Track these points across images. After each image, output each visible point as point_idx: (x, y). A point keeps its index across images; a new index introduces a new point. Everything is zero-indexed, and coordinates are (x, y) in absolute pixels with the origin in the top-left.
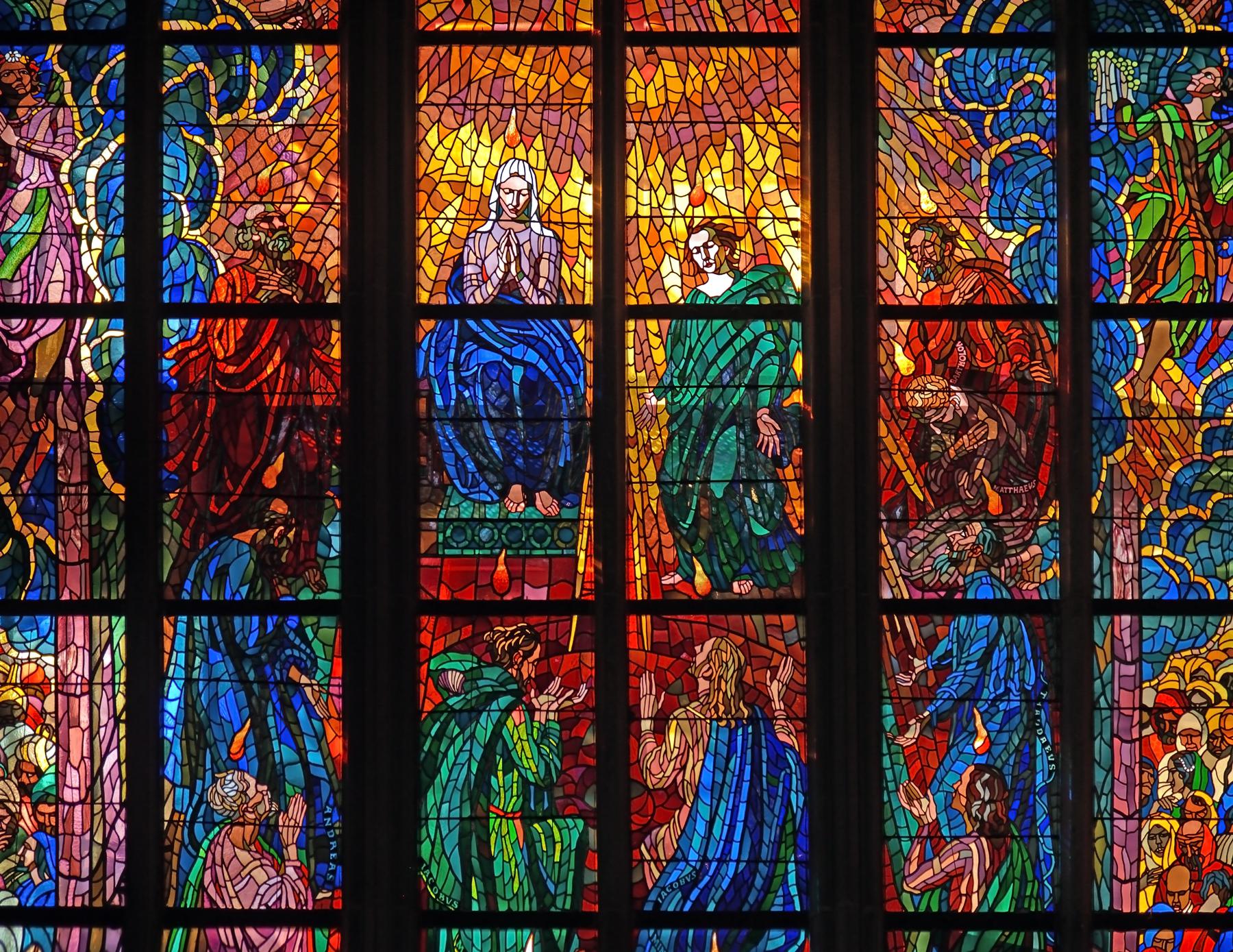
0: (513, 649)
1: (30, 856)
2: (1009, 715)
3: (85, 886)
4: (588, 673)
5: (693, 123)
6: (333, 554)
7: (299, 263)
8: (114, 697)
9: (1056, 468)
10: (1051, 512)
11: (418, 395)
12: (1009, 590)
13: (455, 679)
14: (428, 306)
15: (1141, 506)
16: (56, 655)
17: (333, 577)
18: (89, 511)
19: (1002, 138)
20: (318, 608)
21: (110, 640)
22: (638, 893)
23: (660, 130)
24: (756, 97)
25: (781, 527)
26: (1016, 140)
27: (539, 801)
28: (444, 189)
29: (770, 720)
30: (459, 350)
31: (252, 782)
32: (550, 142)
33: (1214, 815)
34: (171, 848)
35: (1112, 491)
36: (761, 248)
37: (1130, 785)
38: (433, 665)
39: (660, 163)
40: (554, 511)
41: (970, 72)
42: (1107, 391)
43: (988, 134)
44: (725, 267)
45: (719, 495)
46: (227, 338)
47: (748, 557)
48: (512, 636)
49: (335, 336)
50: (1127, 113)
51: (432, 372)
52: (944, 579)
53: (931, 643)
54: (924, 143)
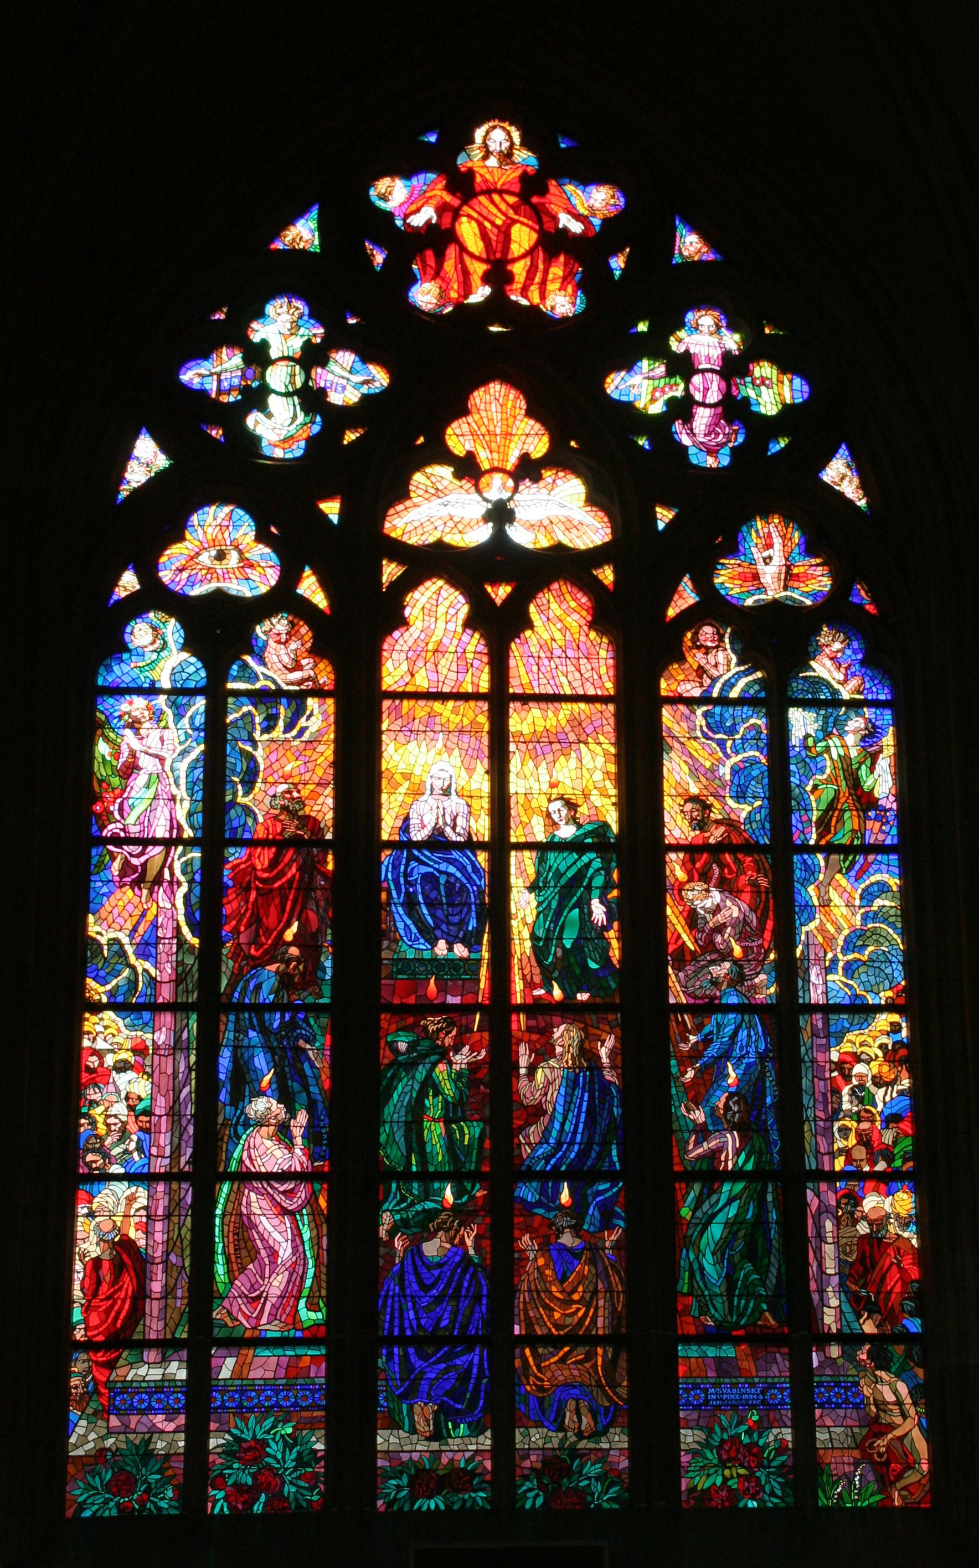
0: (442, 1029)
2: (749, 1066)
4: (485, 1043)
5: (551, 743)
6: (327, 977)
7: (309, 816)
10: (772, 956)
11: (380, 890)
13: (402, 1046)
17: (327, 990)
18: (177, 953)
19: (737, 753)
20: (318, 1009)
21: (187, 1025)
23: (531, 746)
24: (589, 730)
25: (605, 960)
26: (746, 755)
27: (455, 1112)
28: (398, 778)
29: (600, 1067)
30: (407, 865)
31: (274, 1102)
34: (222, 1139)
36: (593, 812)
37: (825, 1102)
41: (718, 718)
43: (729, 751)
45: (568, 946)
46: (263, 858)
47: (585, 980)
48: (439, 1022)
49: (330, 857)
54: (691, 756)
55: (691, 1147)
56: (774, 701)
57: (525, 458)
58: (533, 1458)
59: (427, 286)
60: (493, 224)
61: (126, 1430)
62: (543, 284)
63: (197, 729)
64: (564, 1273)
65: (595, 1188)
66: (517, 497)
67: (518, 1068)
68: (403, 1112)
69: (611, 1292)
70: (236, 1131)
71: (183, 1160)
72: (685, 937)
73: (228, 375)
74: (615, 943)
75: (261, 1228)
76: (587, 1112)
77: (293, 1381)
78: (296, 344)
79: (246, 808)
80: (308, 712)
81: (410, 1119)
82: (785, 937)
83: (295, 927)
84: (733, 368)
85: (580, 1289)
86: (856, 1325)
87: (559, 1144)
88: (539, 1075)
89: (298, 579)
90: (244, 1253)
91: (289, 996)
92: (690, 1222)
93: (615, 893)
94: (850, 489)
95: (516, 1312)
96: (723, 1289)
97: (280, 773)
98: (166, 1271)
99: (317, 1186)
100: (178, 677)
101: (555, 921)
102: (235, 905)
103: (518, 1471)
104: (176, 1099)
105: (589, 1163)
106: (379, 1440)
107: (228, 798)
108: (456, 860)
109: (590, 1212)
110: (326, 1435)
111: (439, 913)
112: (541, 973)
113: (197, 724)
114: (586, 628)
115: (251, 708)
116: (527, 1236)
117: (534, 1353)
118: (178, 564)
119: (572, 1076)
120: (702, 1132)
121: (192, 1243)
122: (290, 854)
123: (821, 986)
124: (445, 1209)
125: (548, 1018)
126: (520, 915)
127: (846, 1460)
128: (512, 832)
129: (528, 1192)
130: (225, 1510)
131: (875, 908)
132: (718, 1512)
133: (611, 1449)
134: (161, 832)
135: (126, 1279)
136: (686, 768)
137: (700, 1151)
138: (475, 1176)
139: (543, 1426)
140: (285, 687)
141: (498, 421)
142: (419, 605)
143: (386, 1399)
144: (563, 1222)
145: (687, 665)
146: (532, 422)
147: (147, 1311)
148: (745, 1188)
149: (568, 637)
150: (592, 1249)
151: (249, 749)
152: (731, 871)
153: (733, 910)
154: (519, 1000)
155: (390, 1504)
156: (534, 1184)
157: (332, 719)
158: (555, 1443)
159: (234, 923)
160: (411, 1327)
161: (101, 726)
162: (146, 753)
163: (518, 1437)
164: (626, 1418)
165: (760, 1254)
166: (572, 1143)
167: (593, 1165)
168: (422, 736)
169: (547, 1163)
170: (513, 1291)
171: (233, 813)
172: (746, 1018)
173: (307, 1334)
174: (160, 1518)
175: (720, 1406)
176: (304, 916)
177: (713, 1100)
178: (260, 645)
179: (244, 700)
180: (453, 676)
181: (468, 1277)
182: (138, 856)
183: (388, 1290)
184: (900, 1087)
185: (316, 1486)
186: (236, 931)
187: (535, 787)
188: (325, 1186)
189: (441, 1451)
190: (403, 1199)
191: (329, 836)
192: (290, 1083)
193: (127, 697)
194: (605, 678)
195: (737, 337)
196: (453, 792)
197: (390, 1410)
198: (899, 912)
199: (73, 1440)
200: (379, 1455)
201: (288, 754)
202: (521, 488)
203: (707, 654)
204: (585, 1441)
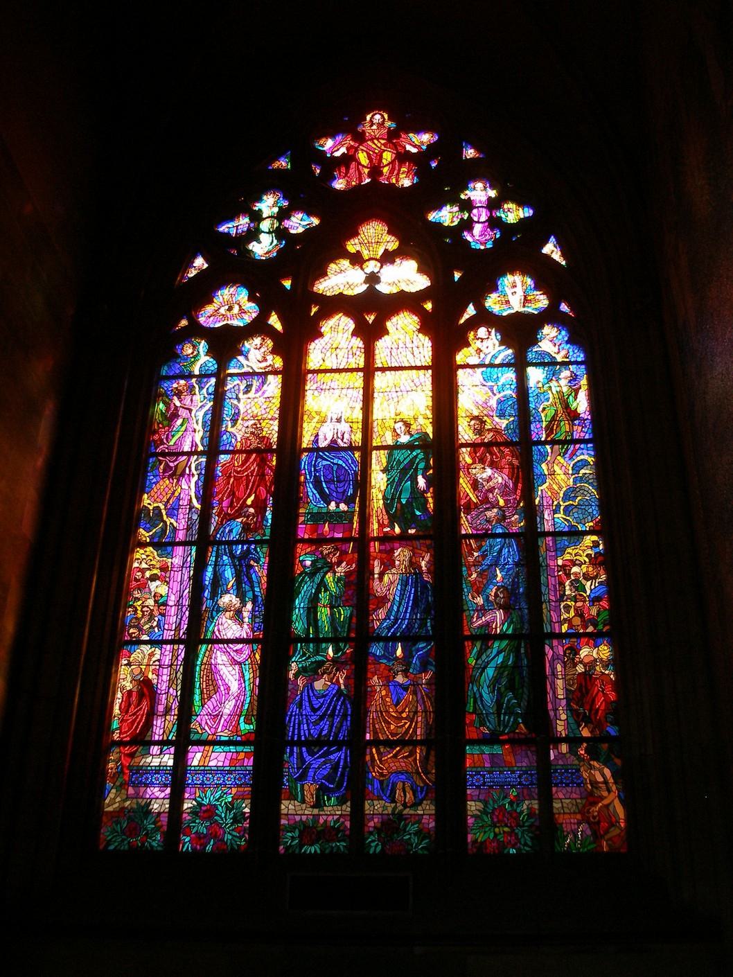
0: (331, 552)
1: (155, 623)
2: (509, 569)
4: (355, 560)
6: (269, 524)
7: (264, 437)
8: (190, 571)
10: (521, 505)
11: (300, 475)
12: (508, 529)
13: (308, 563)
15: (553, 502)
17: (268, 531)
18: (188, 514)
21: (190, 554)
22: (371, 630)
23: (386, 394)
29: (421, 573)
33: (587, 599)
36: (419, 427)
38: (301, 558)
40: (346, 509)
42: (539, 467)
43: (495, 392)
45: (404, 503)
48: (329, 549)
50: (540, 385)
52: (484, 527)
55: (475, 620)
56: (520, 365)
57: (386, 250)
58: (376, 820)
59: (341, 181)
60: (374, 152)
62: (398, 174)
63: (210, 394)
65: (417, 646)
67: (374, 574)
70: (212, 614)
72: (471, 495)
73: (242, 227)
74: (430, 500)
75: (221, 673)
77: (233, 768)
78: (276, 210)
81: (310, 606)
83: (252, 497)
84: (493, 205)
85: (407, 710)
86: (577, 732)
88: (386, 578)
89: (268, 316)
91: (247, 537)
94: (557, 256)
95: (368, 726)
97: (251, 415)
101: (396, 489)
103: (366, 829)
106: (283, 807)
107: (223, 429)
110: (251, 803)
112: (388, 518)
114: (417, 332)
118: (209, 314)
119: (405, 579)
120: (482, 610)
122: (254, 455)
123: (552, 520)
124: (328, 661)
126: (378, 486)
127: (572, 821)
131: (580, 475)
133: (424, 814)
134: (187, 448)
138: (346, 640)
139: (382, 799)
140: (257, 371)
141: (375, 236)
146: (390, 236)
152: (497, 457)
153: (499, 479)
155: (287, 849)
156: (381, 644)
158: (390, 810)
160: (305, 735)
163: (367, 806)
164: (434, 795)
165: (517, 687)
166: (404, 619)
168: (327, 391)
169: (389, 632)
170: (367, 712)
171: (225, 437)
175: (493, 786)
177: (488, 591)
178: (246, 350)
180: (345, 360)
183: (292, 712)
184: (600, 580)
185: (244, 836)
188: (260, 646)
189: (320, 815)
190: (304, 654)
191: (275, 447)
195: (495, 191)
196: (343, 420)
198: (595, 477)
199: (107, 801)
200: (282, 816)
203: (482, 342)
204: (408, 809)
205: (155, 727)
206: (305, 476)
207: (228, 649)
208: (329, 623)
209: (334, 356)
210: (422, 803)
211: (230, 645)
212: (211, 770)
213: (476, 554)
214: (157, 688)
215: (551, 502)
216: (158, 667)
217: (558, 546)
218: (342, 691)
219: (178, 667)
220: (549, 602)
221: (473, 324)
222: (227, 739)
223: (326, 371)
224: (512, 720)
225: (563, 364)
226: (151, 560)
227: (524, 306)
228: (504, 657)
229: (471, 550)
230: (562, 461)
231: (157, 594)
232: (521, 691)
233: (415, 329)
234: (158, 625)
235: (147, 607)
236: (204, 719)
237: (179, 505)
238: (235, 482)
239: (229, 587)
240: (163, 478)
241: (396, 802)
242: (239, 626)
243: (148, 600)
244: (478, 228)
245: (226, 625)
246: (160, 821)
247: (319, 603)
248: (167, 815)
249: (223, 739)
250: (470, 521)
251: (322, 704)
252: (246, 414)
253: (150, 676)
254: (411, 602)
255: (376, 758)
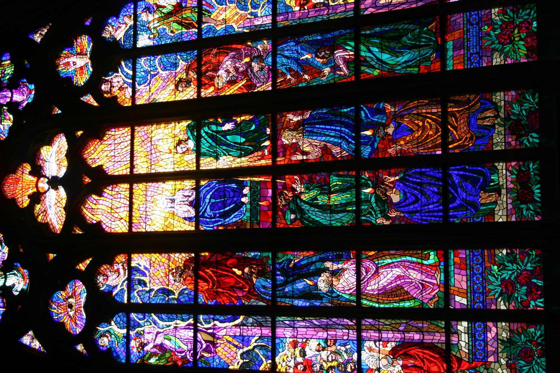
0: (285, 199)
2: (302, 49)
3: (351, 331)
4: (291, 177)
5: (151, 154)
6: (259, 254)
7: (184, 264)
8: (298, 320)
9: (237, 44)
10: (249, 43)
11: (218, 230)
12: (269, 53)
13: (293, 216)
14: (195, 227)
15: (248, 18)
16: (286, 338)
17: (265, 254)
18: (247, 326)
19: (157, 69)
20: (274, 258)
21: (282, 321)
23: (153, 163)
26: (157, 65)
27: (325, 189)
28: (167, 223)
29: (303, 120)
30: (207, 218)
32: (156, 194)
34: (339, 304)
35: (244, 27)
36: (182, 133)
39: (161, 162)
40: (248, 188)
41: (141, 79)
44: (187, 142)
45: (243, 140)
46: (203, 286)
47: (260, 130)
48: (281, 199)
49: (203, 254)
50: (152, 36)
51: (211, 226)
52: (266, 72)
53: (284, 74)
54: (158, 90)
55: (342, 73)
56: (134, 54)
57: (31, 173)
58: (510, 140)
61: (496, 353)
64: (408, 130)
65: (364, 118)
66: (47, 175)
67: (303, 160)
68: (326, 215)
69: (418, 106)
70: (335, 297)
71: (350, 323)
72: (240, 85)
74: (243, 118)
75: (385, 284)
76: (325, 125)
77: (468, 266)
79: (180, 294)
80: (138, 266)
81: (329, 211)
82: (240, 38)
83: (235, 270)
85: (416, 122)
87: (341, 138)
88: (307, 149)
90: (399, 292)
91: (269, 272)
92: (381, 70)
93: (219, 120)
95: (429, 153)
96: (416, 50)
97: (164, 278)
98: (408, 332)
99: (364, 256)
100: (122, 326)
102: (224, 298)
104: (319, 327)
105: (351, 122)
106: (501, 220)
107: (176, 302)
108: (204, 195)
109: (376, 120)
110: (498, 248)
111: (229, 202)
112: (257, 151)
113: (142, 317)
115: (135, 292)
116: (389, 150)
117: (452, 143)
119: (307, 134)
120: (335, 68)
121: (393, 319)
122: (201, 273)
123: (264, 19)
124: (375, 192)
125: (279, 147)
126: (230, 163)
128: (192, 169)
129: (366, 151)
130: (541, 300)
132: (539, 43)
133: (504, 100)
134: (191, 334)
135: (412, 352)
136: (163, 92)
137: (344, 68)
138: (358, 178)
139: (492, 136)
140: (126, 276)
142: (92, 217)
143: (478, 218)
144: (382, 133)
145: (118, 95)
147: (430, 341)
148: (363, 45)
149: (106, 149)
150: (396, 118)
151: (154, 292)
154: (270, 162)
155: (537, 214)
157: (141, 255)
159: (233, 299)
161: (143, 361)
162: (155, 340)
163: (499, 148)
165: (398, 34)
166: (341, 131)
167: (352, 120)
168: (148, 213)
169: (351, 143)
172: (279, 52)
173: (442, 259)
174: (546, 335)
175: (480, 46)
176: (231, 266)
177: (319, 65)
179: (132, 295)
180: (122, 200)
181: (411, 179)
182: (202, 345)
185: (527, 253)
186: (238, 298)
187: (172, 160)
188: (363, 252)
189: (507, 188)
190: (370, 213)
191: (193, 255)
192: (311, 271)
193: (131, 348)
194: (123, 131)
197: (484, 216)
200: (509, 220)
201: (156, 274)
202: (44, 174)
203: (113, 87)
204: (500, 113)
205: (434, 341)
206: (219, 225)
207: (365, 280)
208: (343, 194)
209: (118, 211)
210: (494, 102)
211: (362, 278)
212: (470, 286)
213: (289, 77)
214: (399, 342)
215: (248, 20)
216: (381, 343)
217: (284, 11)
218: (401, 178)
219: (380, 323)
220: (329, 14)
221: (98, 95)
222: (442, 274)
223: (131, 216)
224: (424, 36)
225: (135, 20)
226: (288, 357)
227: (86, 54)
228: (373, 46)
229: (286, 81)
230: (215, 14)
231: (317, 349)
232: (401, 31)
233: (99, 143)
234: (345, 345)
235: (328, 357)
236: (425, 297)
237: (240, 336)
238: (222, 287)
239: (311, 283)
240: (216, 353)
241: (494, 124)
242: (346, 272)
243: (322, 356)
244: (17, 97)
245: (345, 284)
246: (517, 329)
247: (328, 204)
248: (512, 324)
249: (442, 278)
250: (262, 84)
251: (412, 194)
252: (163, 283)
253: (389, 349)
254: (327, 127)
255: (457, 144)
